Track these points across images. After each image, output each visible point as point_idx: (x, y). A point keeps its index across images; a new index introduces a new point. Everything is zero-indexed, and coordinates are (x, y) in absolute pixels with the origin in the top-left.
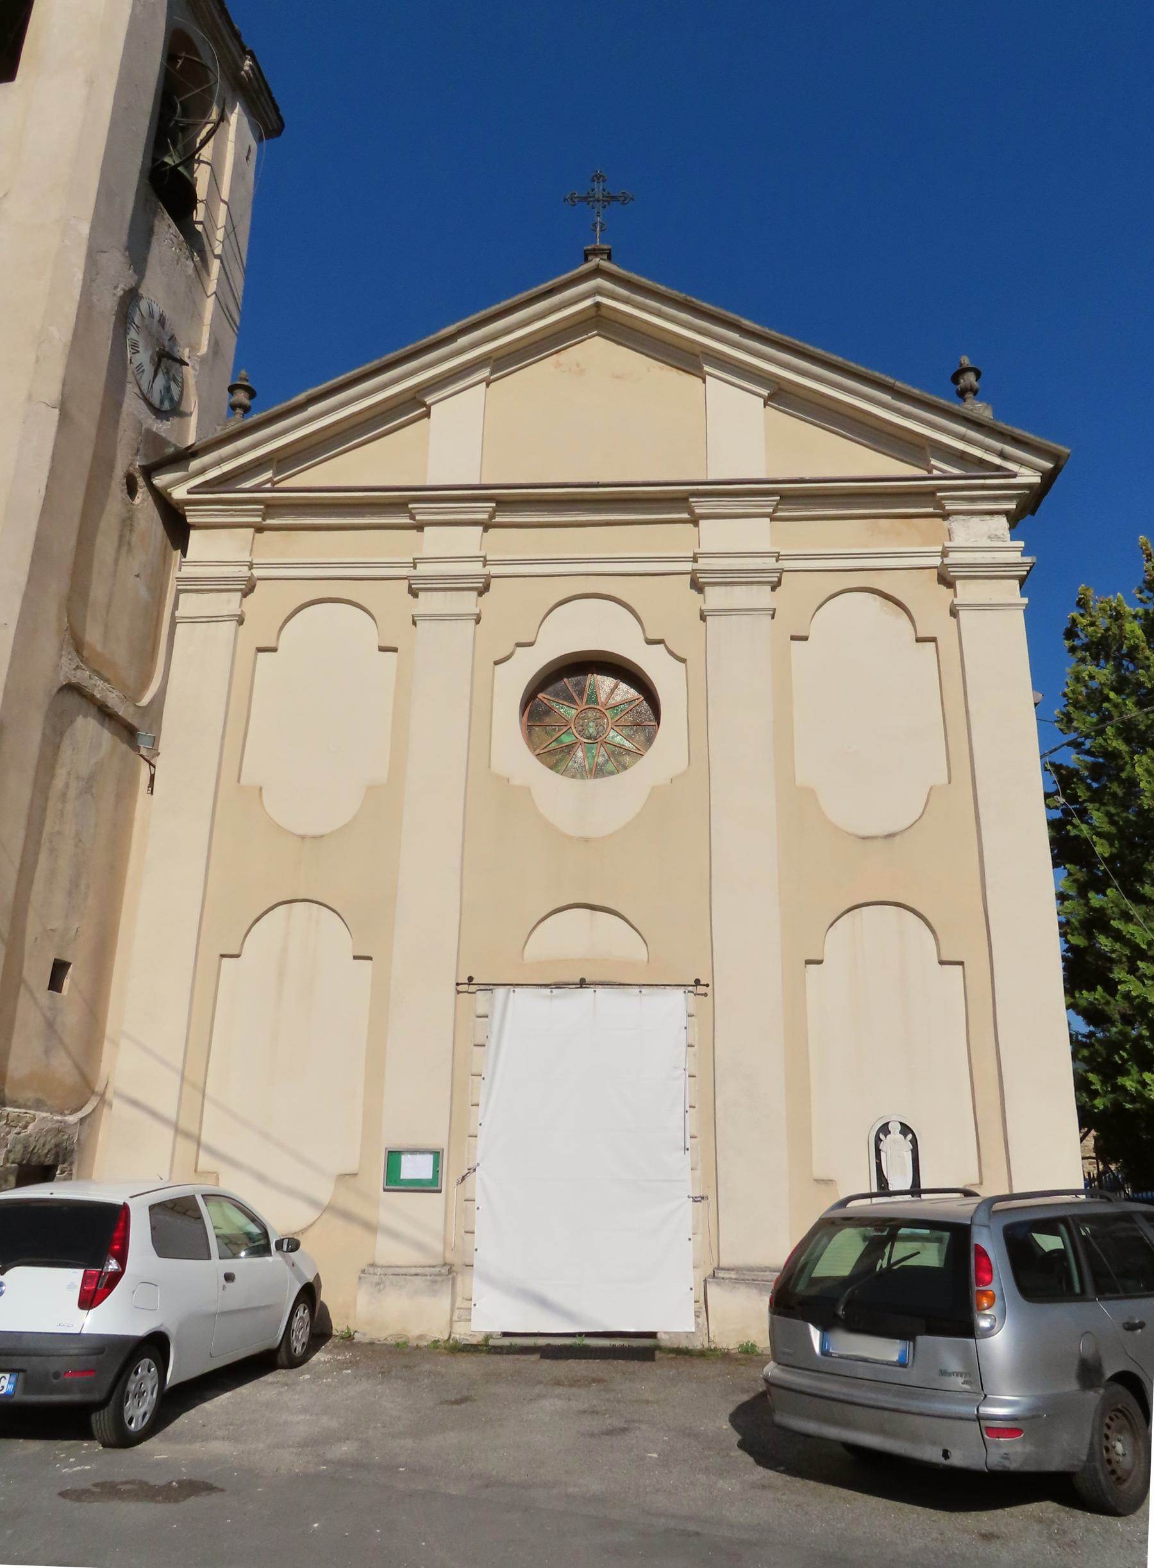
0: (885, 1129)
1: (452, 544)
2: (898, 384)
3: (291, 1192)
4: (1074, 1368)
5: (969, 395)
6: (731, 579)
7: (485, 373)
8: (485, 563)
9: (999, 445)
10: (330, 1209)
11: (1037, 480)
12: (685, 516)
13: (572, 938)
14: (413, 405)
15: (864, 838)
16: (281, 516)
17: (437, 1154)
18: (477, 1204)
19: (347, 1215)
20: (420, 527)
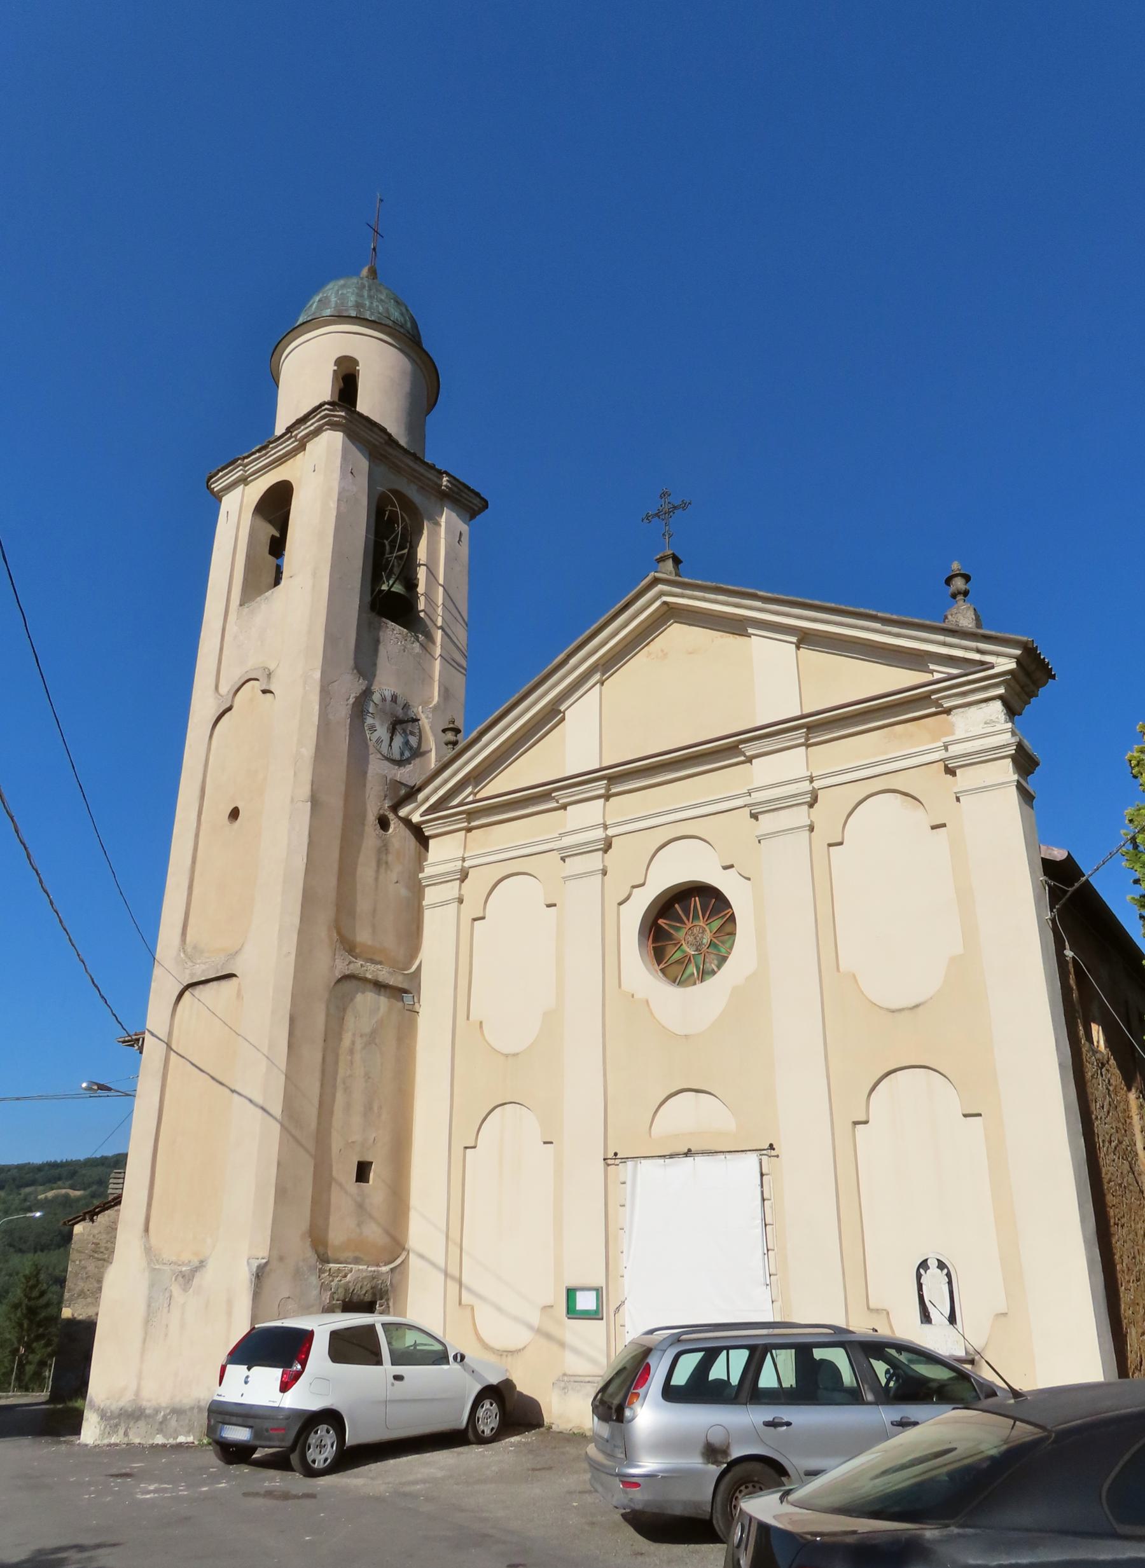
0: (924, 1265)
1: (584, 817)
2: (880, 614)
3: (516, 1319)
4: (700, 1447)
5: (960, 597)
6: (776, 806)
7: (597, 677)
8: (605, 827)
9: (973, 644)
10: (540, 1332)
11: (1013, 665)
12: (742, 758)
13: (684, 1117)
14: (552, 715)
15: (893, 1011)
16: (478, 818)
17: (598, 1290)
18: (627, 1328)
19: (548, 1336)
20: (564, 807)
